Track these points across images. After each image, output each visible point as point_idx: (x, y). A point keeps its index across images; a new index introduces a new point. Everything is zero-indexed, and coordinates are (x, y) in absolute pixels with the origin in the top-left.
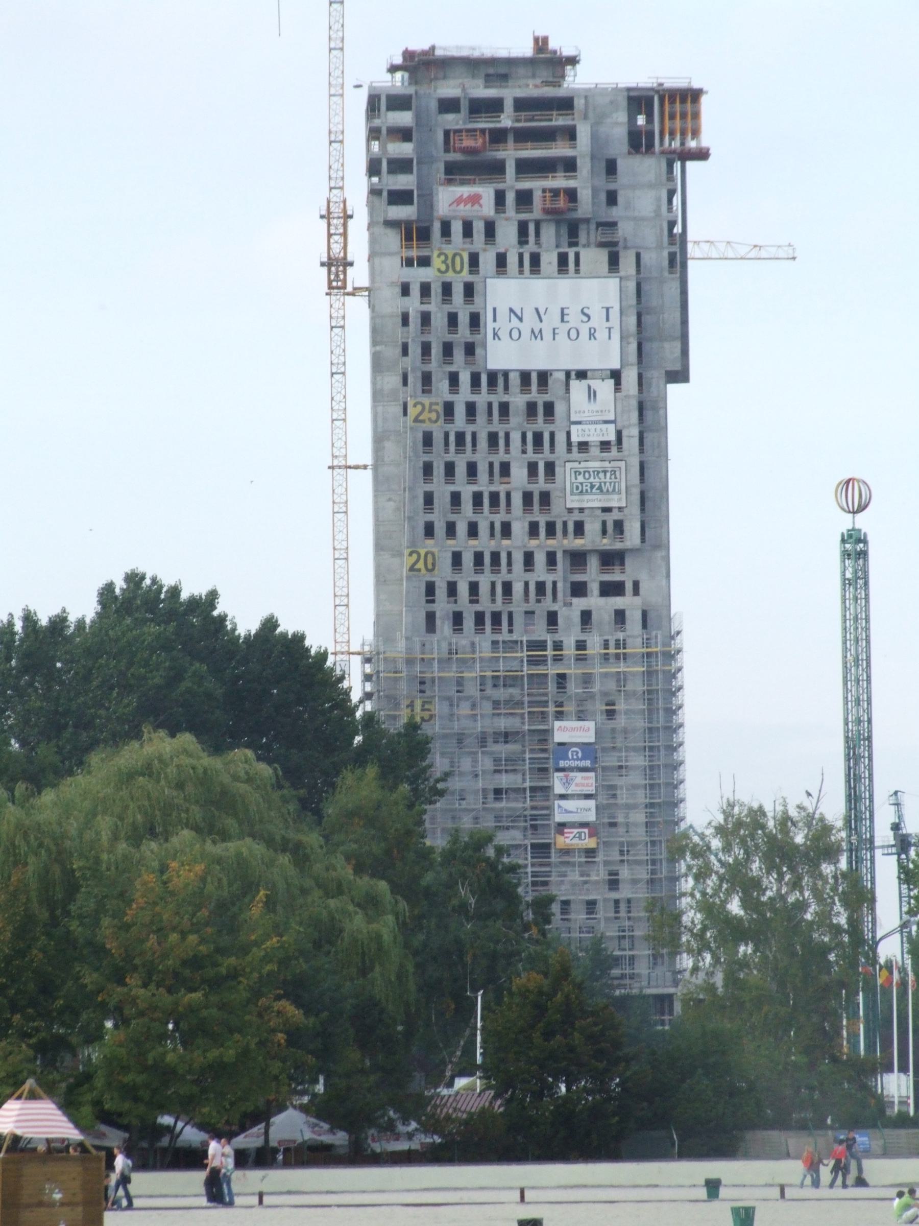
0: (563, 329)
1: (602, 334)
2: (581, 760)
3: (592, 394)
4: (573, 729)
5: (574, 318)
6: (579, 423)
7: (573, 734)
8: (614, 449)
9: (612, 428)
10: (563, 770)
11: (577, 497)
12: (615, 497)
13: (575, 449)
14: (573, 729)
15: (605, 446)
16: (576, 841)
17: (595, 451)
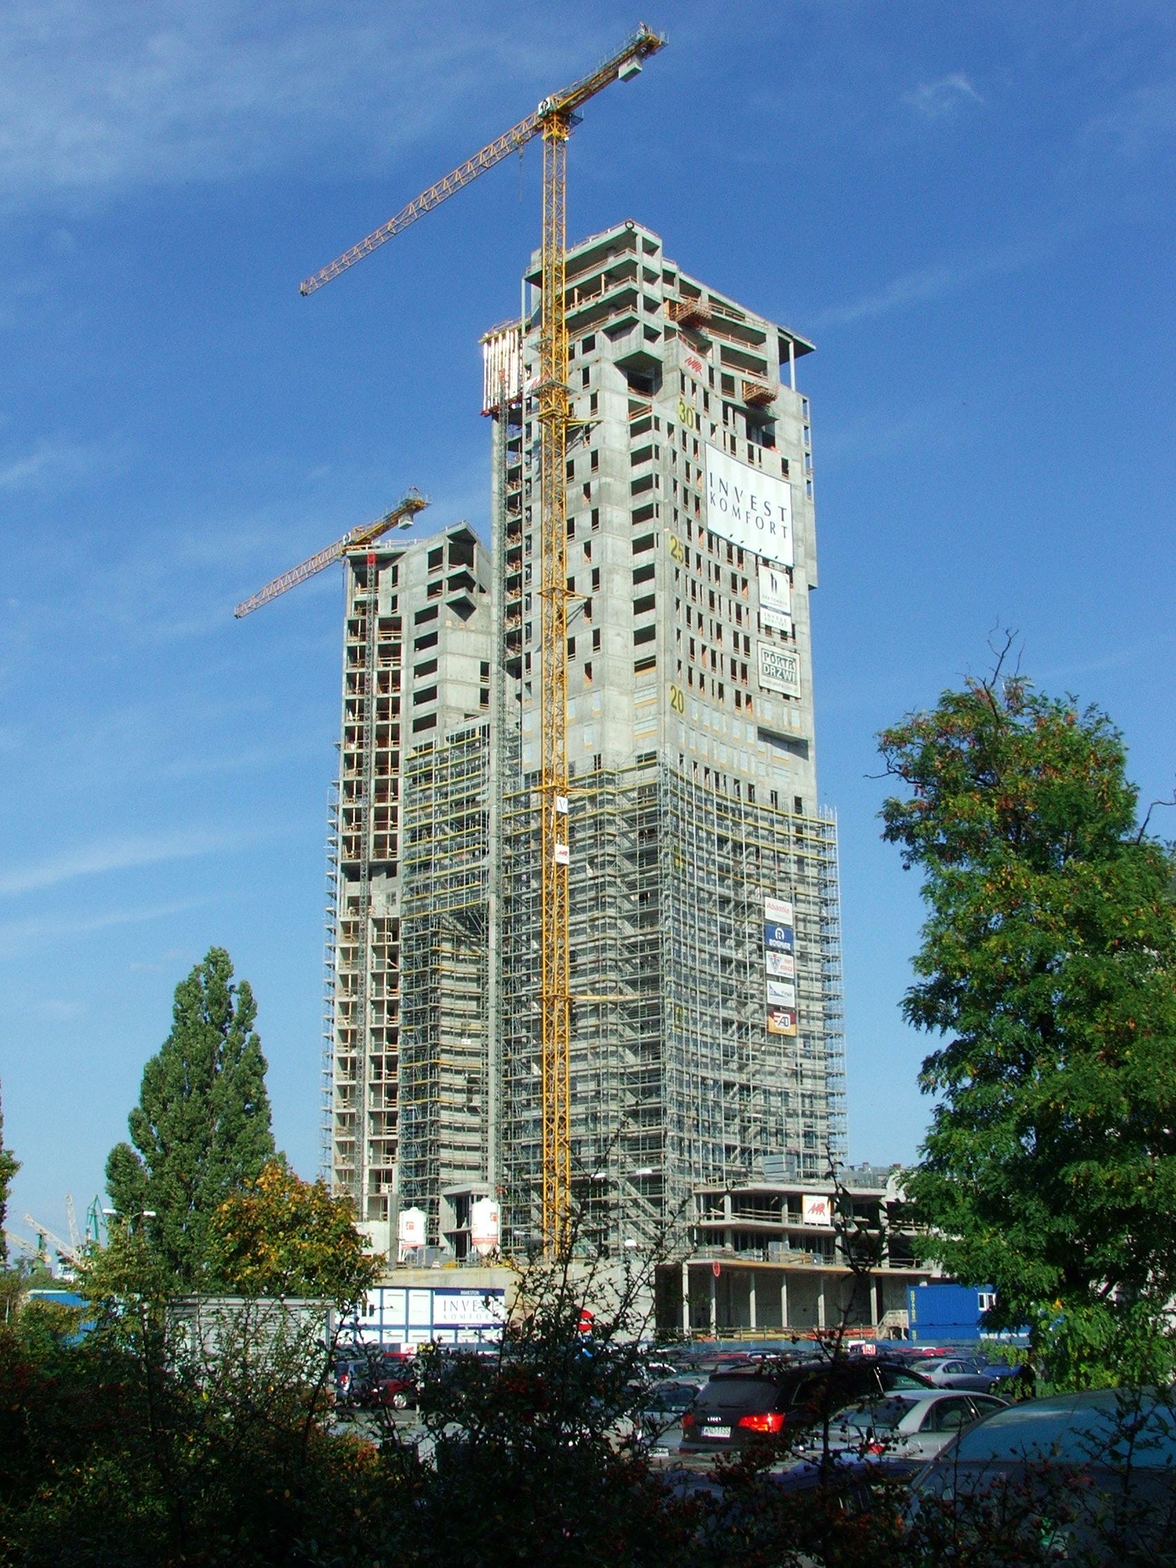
0: (753, 515)
1: (779, 530)
2: (784, 941)
3: (774, 584)
4: (777, 908)
5: (759, 506)
6: (765, 607)
7: (778, 912)
8: (790, 640)
9: (788, 618)
10: (773, 949)
11: (766, 678)
12: (792, 686)
13: (763, 631)
14: (777, 908)
15: (784, 634)
16: (782, 1026)
17: (777, 638)
